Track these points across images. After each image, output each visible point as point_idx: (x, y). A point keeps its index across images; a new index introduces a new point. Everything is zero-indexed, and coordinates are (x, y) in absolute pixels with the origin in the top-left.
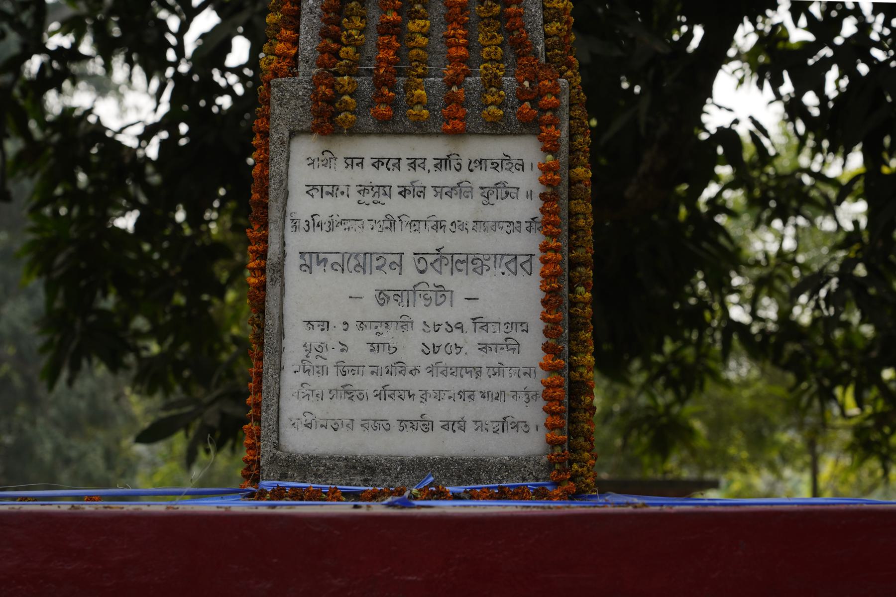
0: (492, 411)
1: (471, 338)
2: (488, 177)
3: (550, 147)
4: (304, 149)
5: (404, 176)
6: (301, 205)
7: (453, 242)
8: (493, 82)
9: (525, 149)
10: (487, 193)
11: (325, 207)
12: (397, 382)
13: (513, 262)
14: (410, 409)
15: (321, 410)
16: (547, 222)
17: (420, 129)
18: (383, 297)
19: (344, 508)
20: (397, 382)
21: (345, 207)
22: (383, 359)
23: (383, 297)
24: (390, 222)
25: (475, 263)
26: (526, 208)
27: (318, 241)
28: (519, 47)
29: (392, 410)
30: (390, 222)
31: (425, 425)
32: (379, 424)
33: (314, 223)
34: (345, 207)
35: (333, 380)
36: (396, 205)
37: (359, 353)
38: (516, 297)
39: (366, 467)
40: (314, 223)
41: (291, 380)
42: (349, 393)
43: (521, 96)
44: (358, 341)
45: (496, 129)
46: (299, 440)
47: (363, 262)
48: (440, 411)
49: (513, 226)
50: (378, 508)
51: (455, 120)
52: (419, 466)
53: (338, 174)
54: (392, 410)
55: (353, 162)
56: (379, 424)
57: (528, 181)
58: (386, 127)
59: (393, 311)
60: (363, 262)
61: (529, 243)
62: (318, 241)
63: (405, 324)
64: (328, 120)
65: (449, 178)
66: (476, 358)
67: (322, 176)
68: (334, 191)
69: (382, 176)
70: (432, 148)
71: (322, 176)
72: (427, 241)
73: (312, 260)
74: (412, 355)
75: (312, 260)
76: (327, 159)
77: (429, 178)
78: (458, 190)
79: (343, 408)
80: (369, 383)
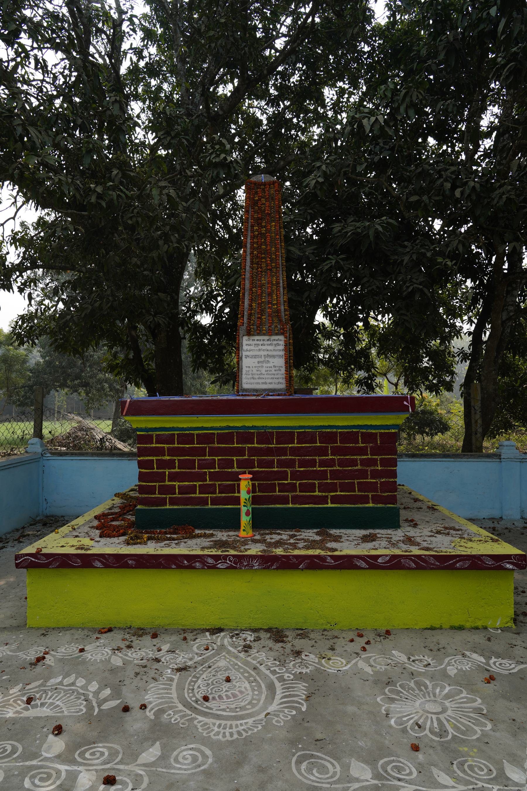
0: (277, 381)
1: (273, 369)
2: (275, 342)
3: (286, 337)
4: (245, 338)
5: (262, 342)
6: (245, 347)
7: (270, 353)
8: (276, 326)
9: (282, 337)
10: (275, 345)
11: (249, 348)
12: (261, 376)
13: (280, 356)
14: (263, 381)
15: (249, 381)
16: (285, 350)
17: (264, 335)
18: (258, 362)
19: (254, 398)
20: (261, 376)
21: (252, 348)
22: (259, 373)
23: (258, 362)
24: (260, 350)
25: (273, 356)
26: (282, 347)
27: (248, 353)
28: (280, 321)
29: (260, 381)
30: (260, 350)
31: (266, 383)
32: (258, 383)
33: (247, 350)
34: (252, 348)
35: (250, 376)
36: (260, 347)
37: (255, 371)
38: (281, 362)
39: (256, 390)
40: (247, 350)
41: (244, 376)
42: (253, 378)
43: (281, 329)
44: (255, 370)
45: (277, 334)
46: (245, 386)
47: (255, 357)
48: (268, 381)
49: (280, 350)
50: (260, 398)
51: (270, 333)
52: (265, 390)
53: (251, 342)
54: (260, 381)
55: (253, 340)
56: (258, 383)
57: (282, 343)
58: (258, 334)
59: (260, 365)
60: (255, 357)
61: (283, 353)
62: (248, 353)
63: (262, 367)
64: (249, 333)
65: (269, 342)
66: (273, 372)
67: (248, 343)
68: (250, 345)
69: (258, 342)
70: (266, 338)
71: (248, 343)
72: (266, 353)
73: (247, 356)
74: (263, 372)
75: (247, 356)
76: (249, 340)
77: (266, 343)
78: (271, 344)
79: (252, 381)
80: (257, 377)
